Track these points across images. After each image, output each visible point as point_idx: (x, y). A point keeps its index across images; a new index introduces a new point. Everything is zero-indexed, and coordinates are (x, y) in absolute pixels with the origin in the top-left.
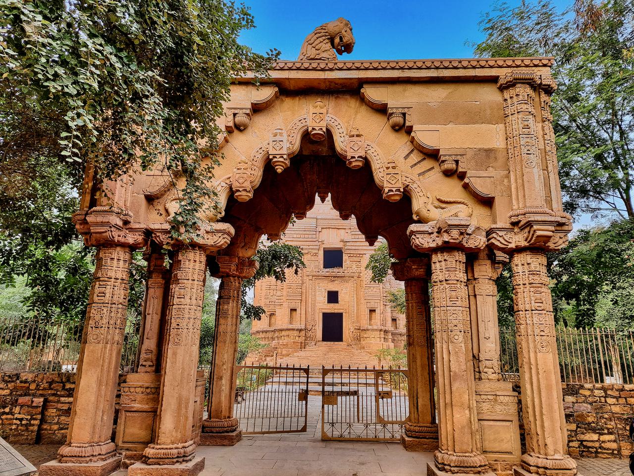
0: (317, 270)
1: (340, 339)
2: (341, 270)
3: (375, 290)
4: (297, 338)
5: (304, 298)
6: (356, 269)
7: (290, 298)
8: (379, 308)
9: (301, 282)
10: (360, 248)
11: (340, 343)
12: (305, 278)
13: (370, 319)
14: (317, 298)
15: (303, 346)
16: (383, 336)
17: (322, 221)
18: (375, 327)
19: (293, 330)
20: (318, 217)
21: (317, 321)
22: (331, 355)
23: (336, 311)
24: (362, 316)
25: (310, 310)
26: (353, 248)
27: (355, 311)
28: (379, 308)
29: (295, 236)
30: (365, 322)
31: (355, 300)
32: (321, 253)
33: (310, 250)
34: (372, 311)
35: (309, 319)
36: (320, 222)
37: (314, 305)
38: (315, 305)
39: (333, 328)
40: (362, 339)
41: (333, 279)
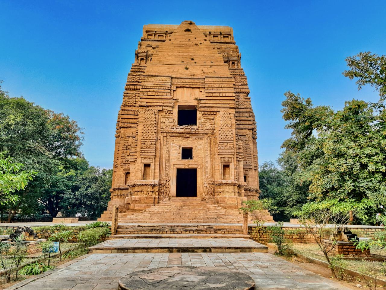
0: (171, 126)
1: (195, 194)
2: (195, 127)
3: (229, 145)
4: (150, 193)
5: (158, 154)
6: (210, 126)
7: (144, 154)
8: (233, 164)
11: (195, 198)
12: (160, 134)
13: (224, 175)
14: (172, 154)
15: (157, 201)
17: (176, 80)
18: (230, 182)
20: (173, 76)
21: (172, 177)
22: (185, 210)
23: (190, 167)
24: (217, 171)
25: (164, 166)
26: (207, 105)
28: (233, 164)
29: (149, 94)
30: (219, 177)
31: (209, 155)
32: (176, 111)
33: (164, 108)
34: (226, 166)
35: (163, 173)
37: (168, 161)
38: (169, 161)
39: (187, 183)
40: (216, 194)
41: (187, 135)
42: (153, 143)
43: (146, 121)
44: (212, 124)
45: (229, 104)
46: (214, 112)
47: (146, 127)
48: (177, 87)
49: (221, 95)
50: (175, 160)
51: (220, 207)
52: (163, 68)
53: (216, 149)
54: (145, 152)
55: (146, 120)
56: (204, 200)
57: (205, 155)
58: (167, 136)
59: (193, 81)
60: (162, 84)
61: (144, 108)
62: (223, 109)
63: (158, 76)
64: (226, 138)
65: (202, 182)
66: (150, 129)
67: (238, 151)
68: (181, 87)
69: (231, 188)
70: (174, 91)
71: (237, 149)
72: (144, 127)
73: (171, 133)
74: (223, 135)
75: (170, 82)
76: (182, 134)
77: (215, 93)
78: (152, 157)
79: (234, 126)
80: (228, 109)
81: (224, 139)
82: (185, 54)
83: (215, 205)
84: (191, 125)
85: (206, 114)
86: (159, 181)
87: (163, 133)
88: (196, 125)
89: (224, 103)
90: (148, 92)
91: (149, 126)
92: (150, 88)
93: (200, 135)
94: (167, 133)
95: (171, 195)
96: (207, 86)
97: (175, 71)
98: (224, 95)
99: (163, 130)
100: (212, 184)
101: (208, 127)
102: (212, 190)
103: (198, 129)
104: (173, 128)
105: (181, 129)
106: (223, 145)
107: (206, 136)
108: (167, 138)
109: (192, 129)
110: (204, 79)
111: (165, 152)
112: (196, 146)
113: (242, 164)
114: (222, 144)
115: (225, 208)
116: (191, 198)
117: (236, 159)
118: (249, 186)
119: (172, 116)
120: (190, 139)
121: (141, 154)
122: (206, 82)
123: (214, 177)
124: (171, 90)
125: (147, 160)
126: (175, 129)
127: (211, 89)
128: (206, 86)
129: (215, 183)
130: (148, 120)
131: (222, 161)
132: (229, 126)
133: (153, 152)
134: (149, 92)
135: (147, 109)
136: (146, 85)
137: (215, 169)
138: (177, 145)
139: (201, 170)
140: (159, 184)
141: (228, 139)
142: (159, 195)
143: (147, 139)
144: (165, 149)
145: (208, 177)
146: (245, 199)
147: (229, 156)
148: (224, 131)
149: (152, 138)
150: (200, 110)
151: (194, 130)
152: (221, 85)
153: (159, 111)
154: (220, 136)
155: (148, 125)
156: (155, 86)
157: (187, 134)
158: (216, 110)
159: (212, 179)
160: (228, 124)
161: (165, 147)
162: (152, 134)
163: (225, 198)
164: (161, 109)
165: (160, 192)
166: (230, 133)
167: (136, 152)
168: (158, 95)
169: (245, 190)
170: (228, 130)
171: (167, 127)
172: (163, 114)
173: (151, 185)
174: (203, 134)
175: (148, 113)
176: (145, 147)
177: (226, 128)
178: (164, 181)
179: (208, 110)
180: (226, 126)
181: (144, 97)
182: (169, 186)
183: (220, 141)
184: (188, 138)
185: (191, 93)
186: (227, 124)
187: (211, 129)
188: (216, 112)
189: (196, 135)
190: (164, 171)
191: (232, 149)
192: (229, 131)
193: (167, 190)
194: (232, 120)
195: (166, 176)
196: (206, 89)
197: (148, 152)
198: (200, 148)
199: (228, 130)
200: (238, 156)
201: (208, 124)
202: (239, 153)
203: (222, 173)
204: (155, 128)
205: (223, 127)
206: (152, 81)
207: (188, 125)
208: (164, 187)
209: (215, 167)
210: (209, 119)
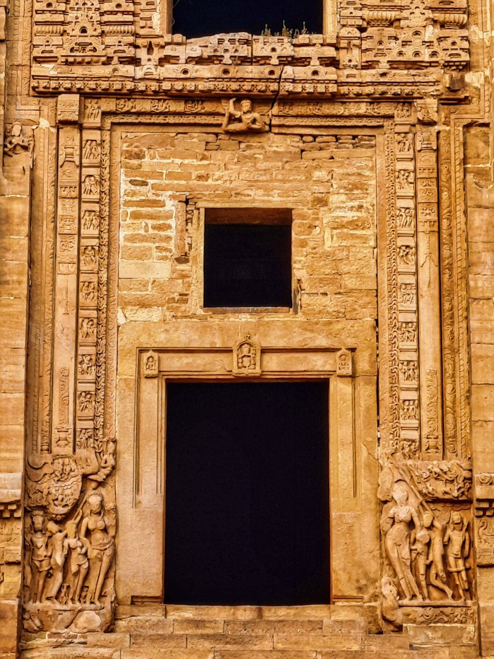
1: (320, 592)
2: (312, 47)
6: (431, 33)
14: (125, 268)
23: (274, 365)
25: (64, 359)
27: (429, 363)
31: (428, 273)
35: (60, 418)
37: (98, 324)
38: (102, 323)
41: (248, 115)
44: (451, 17)
50: (156, 314)
56: (385, 626)
57: (394, 272)
58: (87, 122)
65: (367, 483)
73: (119, 95)
76: (209, 107)
84: (276, 30)
86: (26, 477)
87: (55, 94)
88: (317, 26)
93: (353, 109)
94: (85, 95)
95: (124, 593)
99: (49, 69)
100: (454, 503)
101: (417, 41)
104: (130, 52)
105: (200, 61)
108: (87, 135)
111: (68, 252)
112: (321, 202)
116: (282, 612)
120: (276, 143)
123: (467, 445)
126: (148, 66)
129: (479, 492)
137: (478, 378)
138: (165, 196)
139: (366, 392)
142: (27, 592)
151: (300, 72)
157: (246, 104)
159: (453, 464)
161: (67, 209)
165: (35, 570)
171: (83, 46)
174: (374, 100)
178: (63, 476)
182: (109, 520)
184: (258, 133)
187: (442, 57)
190: (64, 402)
195: (81, 438)
207: (256, 31)
209: (477, 366)
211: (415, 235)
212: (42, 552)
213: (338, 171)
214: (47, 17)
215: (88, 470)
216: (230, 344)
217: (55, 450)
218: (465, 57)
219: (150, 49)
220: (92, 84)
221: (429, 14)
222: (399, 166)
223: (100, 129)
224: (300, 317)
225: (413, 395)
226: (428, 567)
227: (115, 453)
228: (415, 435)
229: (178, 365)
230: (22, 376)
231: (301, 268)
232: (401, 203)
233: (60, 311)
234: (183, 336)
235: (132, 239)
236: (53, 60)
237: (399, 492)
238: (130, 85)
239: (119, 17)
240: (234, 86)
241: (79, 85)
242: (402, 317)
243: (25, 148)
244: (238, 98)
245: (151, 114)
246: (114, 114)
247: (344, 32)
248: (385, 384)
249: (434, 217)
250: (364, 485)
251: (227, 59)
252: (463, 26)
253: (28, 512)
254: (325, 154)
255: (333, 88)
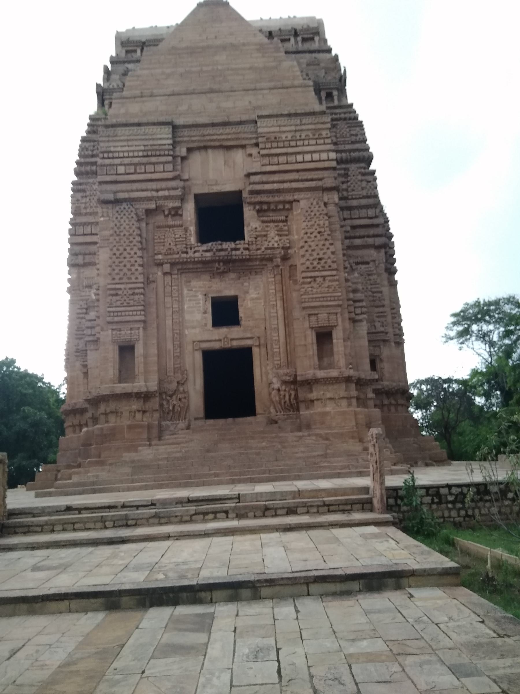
0: (181, 247)
1: (253, 413)
2: (241, 245)
4: (139, 416)
6: (277, 238)
7: (116, 319)
9: (141, 279)
10: (286, 186)
11: (250, 419)
14: (187, 317)
16: (354, 393)
17: (186, 132)
19: (127, 396)
20: (180, 121)
23: (235, 344)
26: (267, 187)
28: (340, 328)
29: (121, 169)
31: (280, 312)
34: (324, 337)
36: (185, 134)
38: (181, 335)
40: (302, 406)
42: (137, 291)
43: (117, 238)
44: (283, 233)
45: (320, 179)
46: (284, 202)
47: (118, 253)
48: (190, 150)
49: (300, 158)
50: (197, 331)
51: (314, 438)
52: (150, 105)
53: (295, 295)
54: (119, 314)
55: (118, 235)
56: (273, 422)
58: (173, 272)
59: (228, 130)
60: (151, 142)
61: (110, 206)
62: (309, 195)
63: (139, 125)
64: (319, 266)
66: (128, 256)
67: (351, 295)
68: (199, 148)
69: (341, 390)
70: (183, 159)
71: (348, 292)
72: (112, 253)
74: (311, 258)
75: (170, 136)
77: (286, 154)
78: (137, 325)
79: (339, 235)
80: (319, 194)
81: (314, 269)
82: (204, 69)
83: (300, 434)
85: (265, 211)
89: (309, 177)
90: (119, 167)
91: (125, 250)
92: (121, 155)
93: (255, 263)
96: (264, 139)
97: (183, 108)
98: (308, 157)
99: (160, 257)
102: (293, 396)
103: (247, 249)
104: (185, 250)
105: (206, 251)
106: (312, 284)
107: (270, 265)
108: (173, 276)
109: (232, 250)
110: (256, 122)
111: (169, 312)
113: (363, 328)
114: (309, 280)
115: (327, 439)
116: (241, 420)
117: (347, 315)
118: (385, 383)
119: (181, 222)
120: (232, 275)
121: (109, 319)
122: (260, 130)
124: (174, 157)
125: (125, 334)
126: (191, 254)
127: (275, 145)
128: (260, 140)
130: (122, 234)
131: (314, 324)
132: (326, 233)
133: (139, 313)
134: (120, 165)
135: (117, 208)
136: (112, 149)
139: (263, 350)
140: (161, 393)
141: (323, 267)
143: (121, 281)
144: (169, 305)
145: (280, 367)
146: (377, 412)
147: (328, 310)
148: (314, 247)
149: (133, 277)
150: (248, 200)
151: (238, 253)
152: (298, 134)
153: (148, 212)
154: (303, 260)
155: (121, 249)
156: (133, 151)
157: (221, 264)
158: (289, 197)
160: (322, 230)
161: (168, 300)
162: (133, 269)
163: (327, 414)
164: (153, 206)
165: (164, 412)
166: (329, 252)
167: (98, 317)
168: (143, 171)
169: (377, 392)
170: (324, 245)
171: (170, 249)
172: (160, 219)
173: (138, 395)
174: (262, 260)
175: (119, 217)
176: (118, 303)
177: (316, 239)
178: (170, 382)
179: (271, 199)
180: (318, 235)
181: (108, 178)
183: (304, 275)
185: (225, 162)
186: (318, 230)
187: (281, 245)
188: (291, 202)
189: (244, 267)
191: (335, 291)
192: (325, 248)
193: (182, 405)
194: (332, 220)
196: (261, 146)
197: (127, 313)
198: (256, 297)
199: (324, 245)
200: (352, 309)
201: (272, 233)
202: (355, 301)
203: (316, 352)
204: (139, 253)
205: (309, 237)
206: (126, 138)
208: (174, 397)
210: (274, 221)
211: (276, 301)
212: (166, 406)
213: (251, 283)
214: (159, 241)
215: (178, 380)
216: (221, 338)
217: (168, 374)
218: (288, 245)
219: (191, 249)
220: (173, 261)
221: (276, 232)
222: (270, 280)
223: (177, 274)
224: (242, 328)
225: (278, 350)
226: (285, 402)
227: (187, 374)
228: (279, 362)
229: (206, 346)
230: (156, 352)
231: (241, 314)
232: (271, 291)
233: (168, 331)
234: (206, 337)
235: (188, 307)
236: (161, 254)
237: (275, 380)
238: (185, 260)
239: (181, 239)
240: (217, 258)
241: (169, 261)
242: (273, 326)
243: (154, 282)
244: (219, 262)
245: (192, 268)
246: (181, 269)
247: (250, 240)
248: (269, 347)
249: (281, 295)
250: (264, 378)
251: (214, 250)
252: (287, 235)
253: (161, 394)
254: (247, 278)
255: (248, 257)
